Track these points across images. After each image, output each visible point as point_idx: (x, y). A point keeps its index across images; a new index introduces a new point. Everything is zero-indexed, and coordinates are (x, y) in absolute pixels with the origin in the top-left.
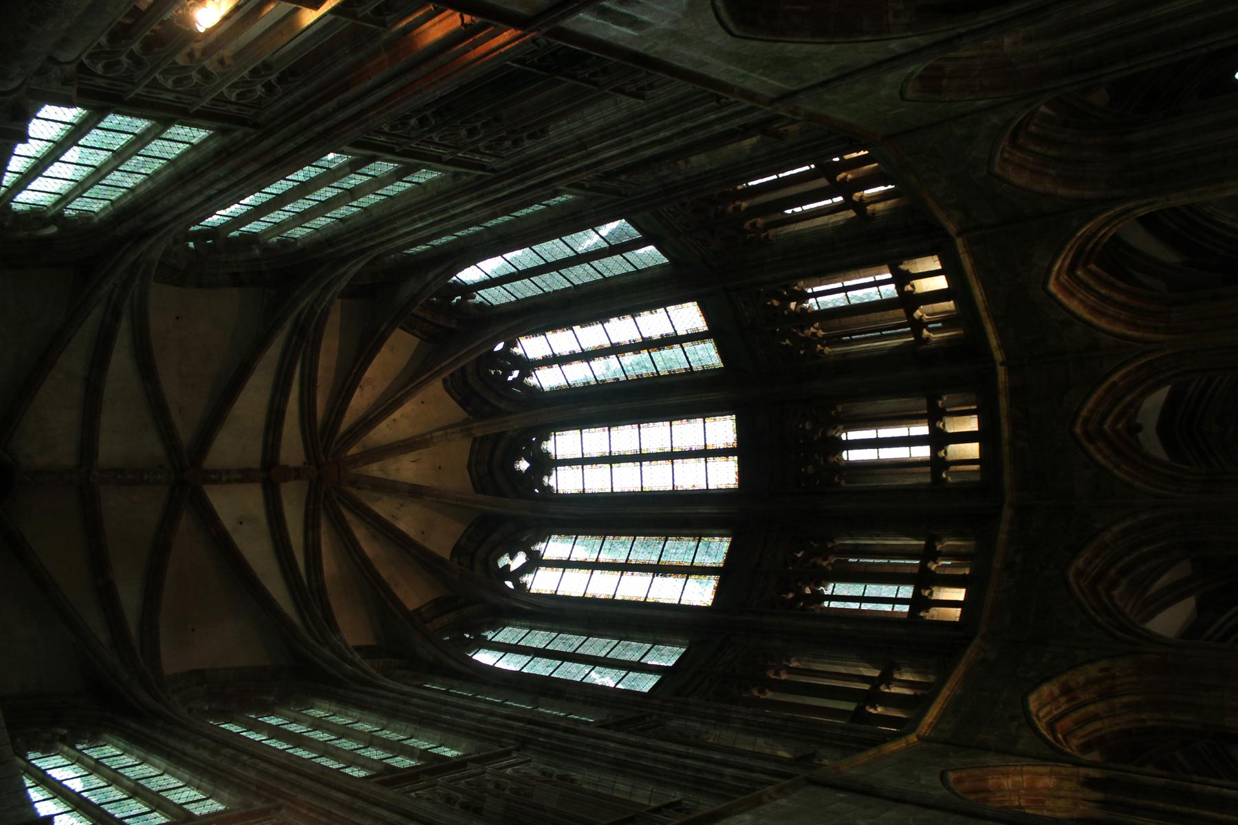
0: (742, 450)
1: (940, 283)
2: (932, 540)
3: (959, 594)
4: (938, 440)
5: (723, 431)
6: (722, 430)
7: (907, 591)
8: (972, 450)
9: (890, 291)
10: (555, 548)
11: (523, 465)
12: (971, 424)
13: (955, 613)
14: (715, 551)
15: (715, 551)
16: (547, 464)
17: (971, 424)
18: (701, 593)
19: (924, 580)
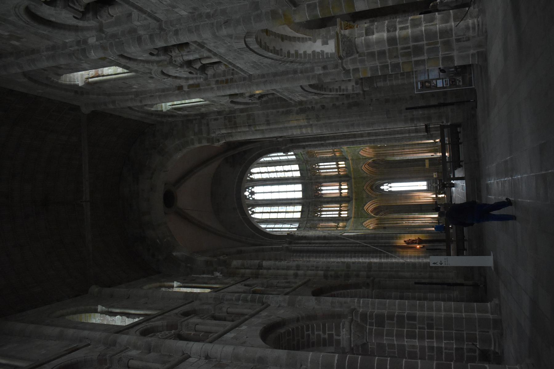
0: (304, 191)
1: (344, 166)
2: (341, 205)
3: (346, 212)
4: (340, 189)
5: (299, 187)
6: (299, 187)
7: (337, 213)
8: (346, 191)
9: (335, 166)
10: (257, 209)
11: (247, 193)
12: (346, 187)
13: (346, 215)
14: (299, 208)
15: (299, 208)
16: (252, 193)
17: (346, 187)
18: (298, 215)
19: (340, 211)
